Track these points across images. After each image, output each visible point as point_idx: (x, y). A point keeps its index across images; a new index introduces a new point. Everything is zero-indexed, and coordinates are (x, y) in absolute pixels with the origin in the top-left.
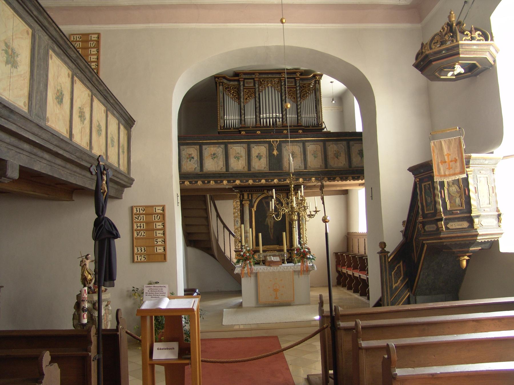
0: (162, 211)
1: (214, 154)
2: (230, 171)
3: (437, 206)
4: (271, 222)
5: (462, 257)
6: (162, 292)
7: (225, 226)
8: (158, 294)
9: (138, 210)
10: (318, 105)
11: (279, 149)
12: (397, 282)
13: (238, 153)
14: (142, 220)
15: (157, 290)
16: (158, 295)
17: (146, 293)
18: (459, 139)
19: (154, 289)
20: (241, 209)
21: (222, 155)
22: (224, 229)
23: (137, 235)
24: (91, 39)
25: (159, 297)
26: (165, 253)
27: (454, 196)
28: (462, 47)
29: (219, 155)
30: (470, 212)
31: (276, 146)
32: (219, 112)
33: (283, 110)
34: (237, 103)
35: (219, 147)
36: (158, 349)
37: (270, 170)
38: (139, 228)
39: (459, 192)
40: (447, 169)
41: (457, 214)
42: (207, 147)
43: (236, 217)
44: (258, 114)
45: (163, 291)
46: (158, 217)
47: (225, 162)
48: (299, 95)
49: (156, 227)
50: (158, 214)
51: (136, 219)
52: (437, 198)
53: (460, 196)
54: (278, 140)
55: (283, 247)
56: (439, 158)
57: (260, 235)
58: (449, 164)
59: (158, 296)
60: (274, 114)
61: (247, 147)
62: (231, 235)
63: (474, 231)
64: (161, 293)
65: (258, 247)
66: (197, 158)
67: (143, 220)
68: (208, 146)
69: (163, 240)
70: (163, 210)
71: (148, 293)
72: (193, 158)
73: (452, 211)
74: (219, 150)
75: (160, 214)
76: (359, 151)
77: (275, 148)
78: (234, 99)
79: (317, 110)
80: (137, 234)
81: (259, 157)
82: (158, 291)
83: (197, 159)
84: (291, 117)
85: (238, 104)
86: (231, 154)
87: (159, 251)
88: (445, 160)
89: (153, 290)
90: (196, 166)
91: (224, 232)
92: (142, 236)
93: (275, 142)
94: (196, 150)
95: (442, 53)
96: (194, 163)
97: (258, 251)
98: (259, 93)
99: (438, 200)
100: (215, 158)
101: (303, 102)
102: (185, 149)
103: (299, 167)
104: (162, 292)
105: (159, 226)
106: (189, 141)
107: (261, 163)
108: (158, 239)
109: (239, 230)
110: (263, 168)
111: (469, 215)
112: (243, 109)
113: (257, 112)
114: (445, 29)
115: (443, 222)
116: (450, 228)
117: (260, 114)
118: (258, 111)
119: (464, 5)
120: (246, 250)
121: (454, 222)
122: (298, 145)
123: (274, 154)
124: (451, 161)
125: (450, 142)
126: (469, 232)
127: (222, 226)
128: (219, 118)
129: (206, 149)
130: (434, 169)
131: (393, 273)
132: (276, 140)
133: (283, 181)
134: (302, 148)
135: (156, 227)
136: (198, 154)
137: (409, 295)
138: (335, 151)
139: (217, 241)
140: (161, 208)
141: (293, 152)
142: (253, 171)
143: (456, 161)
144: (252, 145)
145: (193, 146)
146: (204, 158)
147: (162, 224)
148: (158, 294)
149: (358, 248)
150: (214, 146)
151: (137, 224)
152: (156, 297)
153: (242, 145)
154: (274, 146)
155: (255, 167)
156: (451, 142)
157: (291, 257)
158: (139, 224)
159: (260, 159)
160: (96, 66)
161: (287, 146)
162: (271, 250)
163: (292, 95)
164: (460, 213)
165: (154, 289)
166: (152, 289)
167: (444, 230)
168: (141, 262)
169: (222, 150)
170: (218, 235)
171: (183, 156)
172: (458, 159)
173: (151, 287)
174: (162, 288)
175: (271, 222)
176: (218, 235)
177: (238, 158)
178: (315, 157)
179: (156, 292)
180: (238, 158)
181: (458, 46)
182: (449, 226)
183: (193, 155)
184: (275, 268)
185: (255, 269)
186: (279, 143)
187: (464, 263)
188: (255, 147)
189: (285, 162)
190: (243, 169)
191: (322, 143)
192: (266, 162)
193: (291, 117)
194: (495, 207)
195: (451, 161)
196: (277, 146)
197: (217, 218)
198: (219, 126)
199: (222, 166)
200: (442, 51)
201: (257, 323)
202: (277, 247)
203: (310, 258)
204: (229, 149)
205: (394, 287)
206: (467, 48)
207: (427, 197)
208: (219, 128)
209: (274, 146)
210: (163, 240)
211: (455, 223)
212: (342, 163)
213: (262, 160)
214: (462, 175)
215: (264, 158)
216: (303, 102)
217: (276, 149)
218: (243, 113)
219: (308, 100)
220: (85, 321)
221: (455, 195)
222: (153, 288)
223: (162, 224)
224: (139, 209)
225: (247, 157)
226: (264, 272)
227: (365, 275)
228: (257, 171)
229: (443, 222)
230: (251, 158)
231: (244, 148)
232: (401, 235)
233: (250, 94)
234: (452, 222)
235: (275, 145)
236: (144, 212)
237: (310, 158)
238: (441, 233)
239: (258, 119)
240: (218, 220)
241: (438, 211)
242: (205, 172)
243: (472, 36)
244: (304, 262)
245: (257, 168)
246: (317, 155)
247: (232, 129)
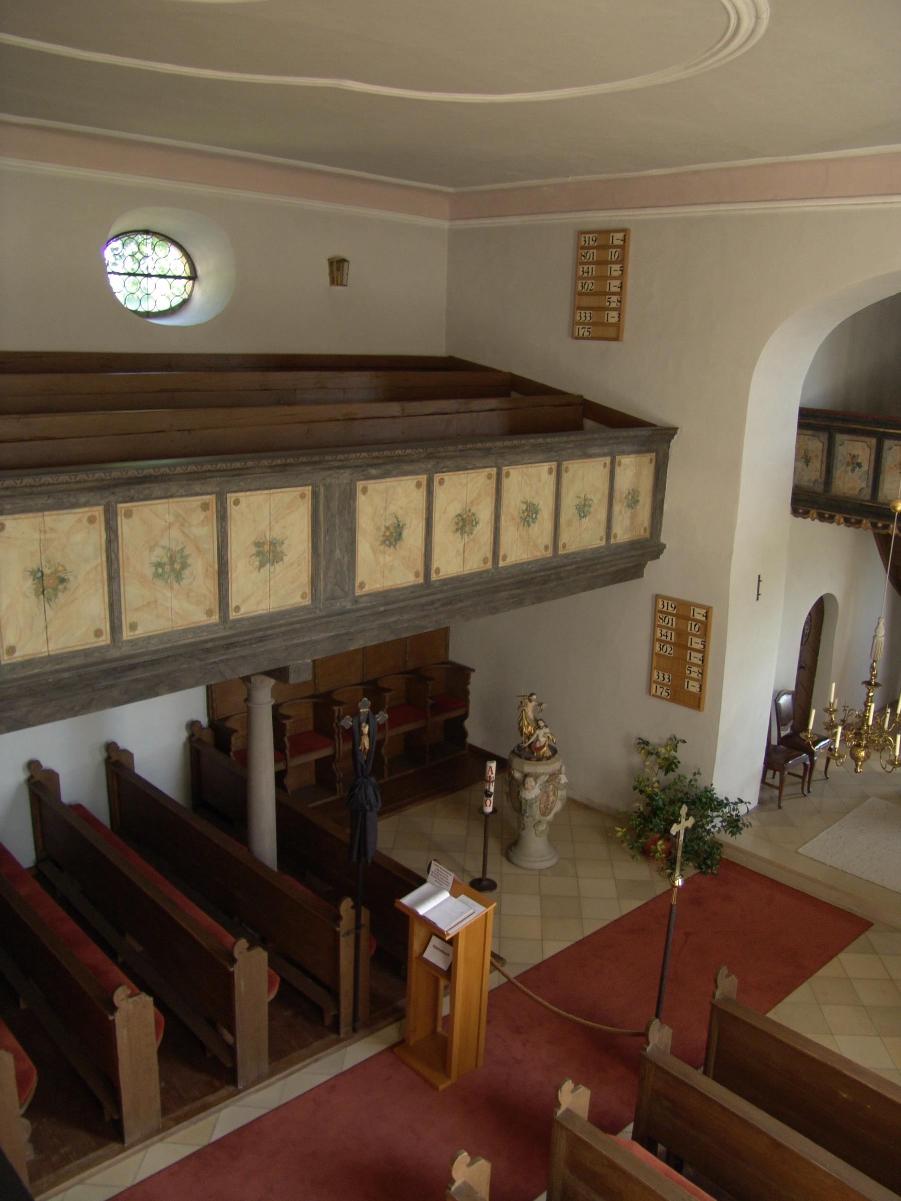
9: (666, 605)
14: (670, 625)
23: (659, 649)
24: (612, 243)
36: (434, 946)
38: (664, 638)
42: (895, 445)
50: (697, 621)
51: (661, 621)
66: (869, 466)
67: (672, 625)
68: (896, 442)
69: (700, 671)
72: (859, 465)
80: (660, 647)
83: (867, 468)
87: (691, 689)
90: (863, 485)
92: (667, 654)
96: (860, 478)
102: (846, 442)
108: (693, 668)
129: (890, 449)
136: (873, 457)
140: (703, 612)
145: (863, 438)
146: (882, 470)
151: (662, 631)
158: (664, 631)
160: (619, 304)
168: (660, 697)
171: (840, 458)
183: (860, 457)
210: (700, 671)
220: (489, 809)
222: (439, 869)
224: (668, 603)
236: (675, 612)
242: (880, 503)
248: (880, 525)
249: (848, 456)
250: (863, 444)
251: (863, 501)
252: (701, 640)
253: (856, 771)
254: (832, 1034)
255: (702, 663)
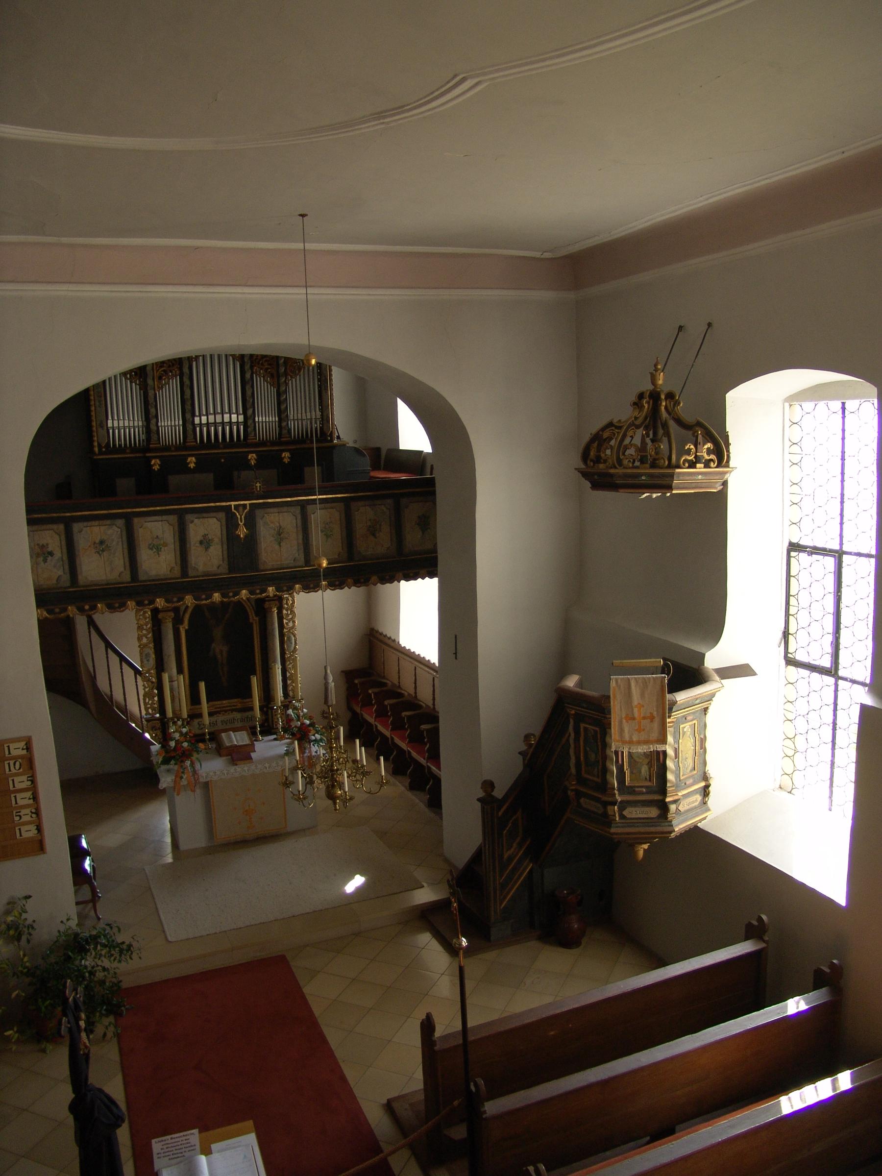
0: (26, 750)
1: (102, 542)
2: (142, 577)
3: (608, 777)
4: (221, 651)
5: (637, 845)
6: (189, 1145)
7: (108, 645)
8: (181, 1151)
10: (325, 389)
11: (251, 522)
12: (511, 847)
13: (157, 537)
15: (179, 1143)
16: (182, 1153)
17: (158, 1154)
18: (662, 680)
19: (172, 1143)
20: (155, 629)
21: (120, 543)
22: (107, 654)
25: (184, 1156)
26: (40, 838)
27: (638, 762)
28: (678, 477)
29: (114, 543)
30: (663, 792)
31: (243, 516)
32: (93, 408)
33: (248, 406)
34: (138, 387)
35: (113, 524)
37: (231, 570)
39: (649, 755)
40: (637, 730)
41: (642, 793)
42: (84, 527)
43: (145, 645)
44: (188, 416)
45: (189, 1143)
46: (18, 764)
47: (127, 559)
48: (282, 370)
49: (14, 787)
50: (15, 758)
52: (608, 764)
53: (650, 764)
54: (247, 502)
55: (252, 701)
56: (623, 710)
57: (202, 685)
58: (641, 722)
59: (183, 1155)
60: (226, 417)
61: (178, 521)
62: (124, 664)
63: (667, 824)
64: (187, 1147)
65: (197, 707)
68: (85, 524)
69: (34, 811)
70: (29, 748)
71: (161, 1153)
72: (51, 554)
73: (634, 789)
74: (113, 532)
75: (22, 757)
76: (419, 517)
77: (241, 522)
78: (128, 376)
79: (321, 401)
81: (205, 543)
82: (181, 1144)
83: (60, 555)
84: (266, 419)
85: (140, 389)
86: (141, 539)
87: (25, 835)
88: (634, 716)
89: (170, 1146)
90: (60, 572)
91: (107, 657)
93: (241, 509)
94: (58, 534)
95: (640, 479)
96: (55, 567)
97: (200, 715)
98: (189, 363)
99: (611, 766)
100: (103, 551)
101: (290, 382)
103: (294, 560)
104: (189, 1145)
105: (22, 782)
106: (40, 516)
107: (210, 557)
109: (151, 673)
110: (215, 568)
111: (660, 798)
112: (152, 403)
113: (187, 411)
114: (645, 407)
115: (616, 807)
116: (628, 817)
117: (194, 415)
118: (190, 407)
119: (678, 334)
120: (181, 733)
121: (635, 806)
122: (290, 512)
123: (239, 536)
124: (643, 717)
125: (645, 683)
126: (660, 825)
127: (103, 645)
128: (94, 424)
129: (81, 531)
130: (612, 729)
131: (504, 832)
132: (242, 503)
133: (261, 593)
134: (299, 517)
135: (14, 787)
136: (64, 543)
137: (531, 872)
138: (370, 520)
139: (93, 679)
141: (280, 527)
142: (192, 575)
143: (652, 718)
144: (189, 517)
146: (77, 553)
147: (28, 777)
148: (181, 1151)
149: (397, 677)
150: (101, 522)
152: (178, 1157)
153: (165, 517)
154: (239, 517)
155: (196, 567)
156: (648, 683)
157: (267, 720)
159: (207, 549)
161: (266, 515)
162: (226, 711)
163: (268, 368)
164: (647, 793)
165: (172, 1143)
166: (168, 1144)
167: (617, 819)
169: (119, 532)
170: (94, 666)
172: (656, 716)
173: (165, 1140)
174: (188, 1137)
175: (221, 651)
176: (94, 666)
177: (157, 548)
178: (327, 536)
179: (177, 1148)
180: (158, 548)
181: (672, 476)
182: (625, 813)
184: (246, 768)
185: (204, 775)
186: (250, 510)
187: (641, 853)
188: (196, 521)
189: (263, 550)
190: (170, 571)
191: (341, 505)
192: (220, 553)
193: (266, 419)
194: (701, 773)
195: (644, 718)
196: (244, 517)
197: (89, 629)
198: (96, 444)
199: (122, 569)
200: (642, 476)
201: (239, 927)
202: (236, 702)
203: (316, 741)
204: (135, 528)
205: (506, 857)
206: (688, 478)
207: (588, 749)
208: (96, 449)
209: (239, 517)
210: (34, 811)
211: (637, 809)
212: (383, 546)
213: (212, 549)
214: (660, 746)
215: (217, 544)
216: (290, 382)
217: (244, 524)
218: (154, 414)
219: (302, 376)
221: (641, 761)
223: (29, 779)
225: (178, 544)
226: (221, 779)
227: (424, 759)
228: (203, 576)
229: (616, 807)
230: (188, 546)
231: (170, 524)
232: (520, 760)
233: (169, 366)
234: (632, 806)
235: (241, 517)
237: (317, 539)
238: (612, 823)
239: (189, 427)
240: (92, 633)
241: (609, 786)
242: (83, 586)
243: (698, 454)
244: (305, 749)
245: (201, 568)
246: (331, 531)
247: (128, 451)
248: (87, 607)
249: (36, 547)
250: (51, 532)
251: (65, 588)
252: (26, 776)
253: (336, 810)
254: (390, 1041)
255: (34, 801)
